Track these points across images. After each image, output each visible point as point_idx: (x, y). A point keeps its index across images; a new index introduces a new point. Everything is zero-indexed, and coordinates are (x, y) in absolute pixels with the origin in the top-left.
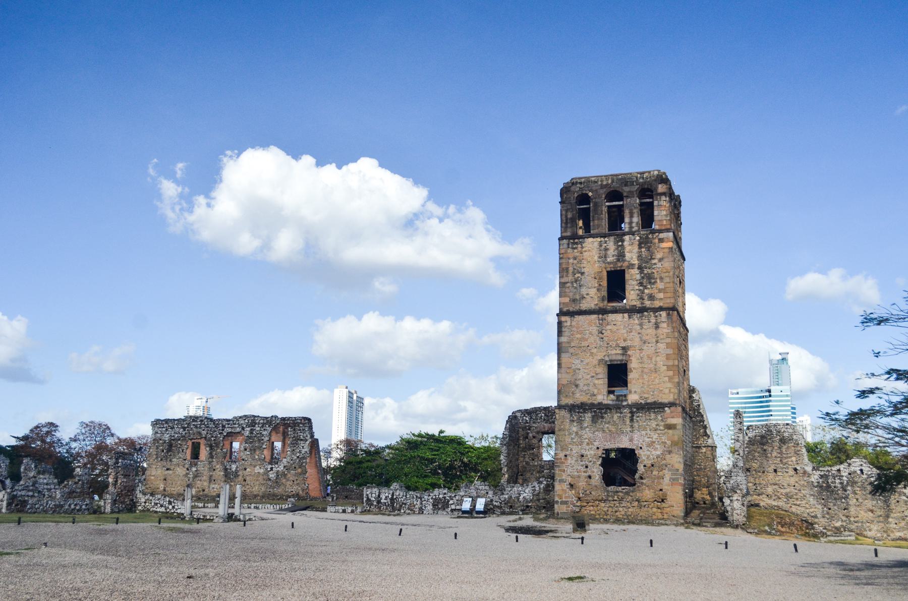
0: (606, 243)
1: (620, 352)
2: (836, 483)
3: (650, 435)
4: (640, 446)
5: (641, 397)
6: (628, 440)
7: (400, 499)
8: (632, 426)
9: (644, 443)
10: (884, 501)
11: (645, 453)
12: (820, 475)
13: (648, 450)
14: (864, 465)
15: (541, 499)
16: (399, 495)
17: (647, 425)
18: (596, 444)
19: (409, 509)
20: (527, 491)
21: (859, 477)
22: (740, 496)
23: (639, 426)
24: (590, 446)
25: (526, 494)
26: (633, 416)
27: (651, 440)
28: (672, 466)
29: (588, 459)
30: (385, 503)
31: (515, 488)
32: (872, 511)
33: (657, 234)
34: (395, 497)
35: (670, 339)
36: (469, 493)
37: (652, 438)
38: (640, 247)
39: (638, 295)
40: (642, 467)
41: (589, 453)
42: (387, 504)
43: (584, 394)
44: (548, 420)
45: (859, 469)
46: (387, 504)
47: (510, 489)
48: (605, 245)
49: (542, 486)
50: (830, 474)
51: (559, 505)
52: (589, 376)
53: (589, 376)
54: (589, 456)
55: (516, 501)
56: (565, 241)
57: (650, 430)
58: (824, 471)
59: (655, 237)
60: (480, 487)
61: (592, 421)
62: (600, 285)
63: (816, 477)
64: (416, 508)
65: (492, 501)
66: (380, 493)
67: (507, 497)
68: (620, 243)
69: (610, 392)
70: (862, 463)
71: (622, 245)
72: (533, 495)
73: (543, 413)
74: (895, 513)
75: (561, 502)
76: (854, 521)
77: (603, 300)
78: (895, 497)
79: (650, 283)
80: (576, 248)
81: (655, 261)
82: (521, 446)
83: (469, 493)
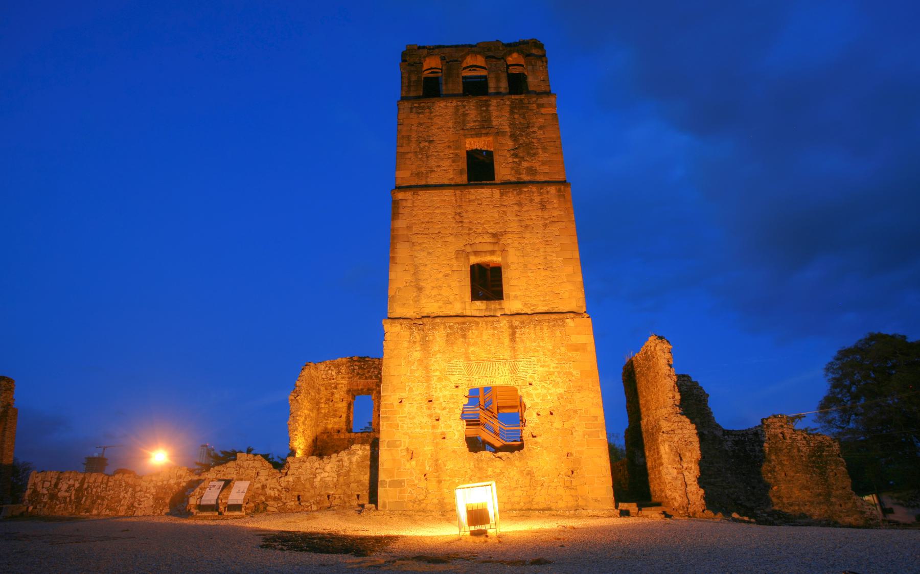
0: (464, 108)
1: (490, 240)
2: (755, 451)
3: (544, 362)
4: (529, 380)
5: (526, 304)
6: (508, 372)
7: (94, 490)
8: (513, 349)
9: (536, 375)
10: (820, 474)
11: (539, 391)
12: (734, 440)
13: (543, 387)
14: (786, 426)
15: (353, 482)
16: (95, 482)
17: (539, 346)
18: (454, 379)
19: (108, 507)
20: (328, 468)
21: (783, 443)
22: (691, 461)
23: (525, 348)
24: (443, 384)
25: (327, 474)
26: (513, 334)
27: (546, 369)
28: (586, 411)
29: (441, 404)
30: (65, 498)
31: (308, 464)
32: (807, 488)
33: (535, 99)
34: (86, 486)
35: (564, 223)
36: (224, 475)
37: (548, 366)
38: (512, 112)
39: (512, 168)
40: (535, 415)
41: (441, 394)
42: (68, 499)
43: (433, 301)
44: (364, 374)
45: (780, 431)
46: (68, 499)
47: (297, 465)
48: (464, 110)
49: (355, 459)
50: (747, 439)
51: (388, 488)
52: (440, 275)
53: (440, 275)
54: (441, 400)
55: (308, 486)
56: (407, 105)
57: (545, 354)
58: (739, 435)
59: (531, 102)
60: (246, 464)
61: (447, 341)
62: (457, 155)
63: (730, 443)
64: (123, 505)
65: (264, 487)
66: (59, 479)
67: (291, 479)
68: (484, 109)
69: (475, 296)
70: (782, 424)
71: (487, 110)
72: (339, 475)
73: (356, 365)
74: (837, 490)
75: (390, 482)
76: (788, 503)
77: (461, 173)
78: (833, 468)
79: (528, 154)
80: (422, 113)
81: (535, 129)
82: (323, 411)
83: (224, 475)
